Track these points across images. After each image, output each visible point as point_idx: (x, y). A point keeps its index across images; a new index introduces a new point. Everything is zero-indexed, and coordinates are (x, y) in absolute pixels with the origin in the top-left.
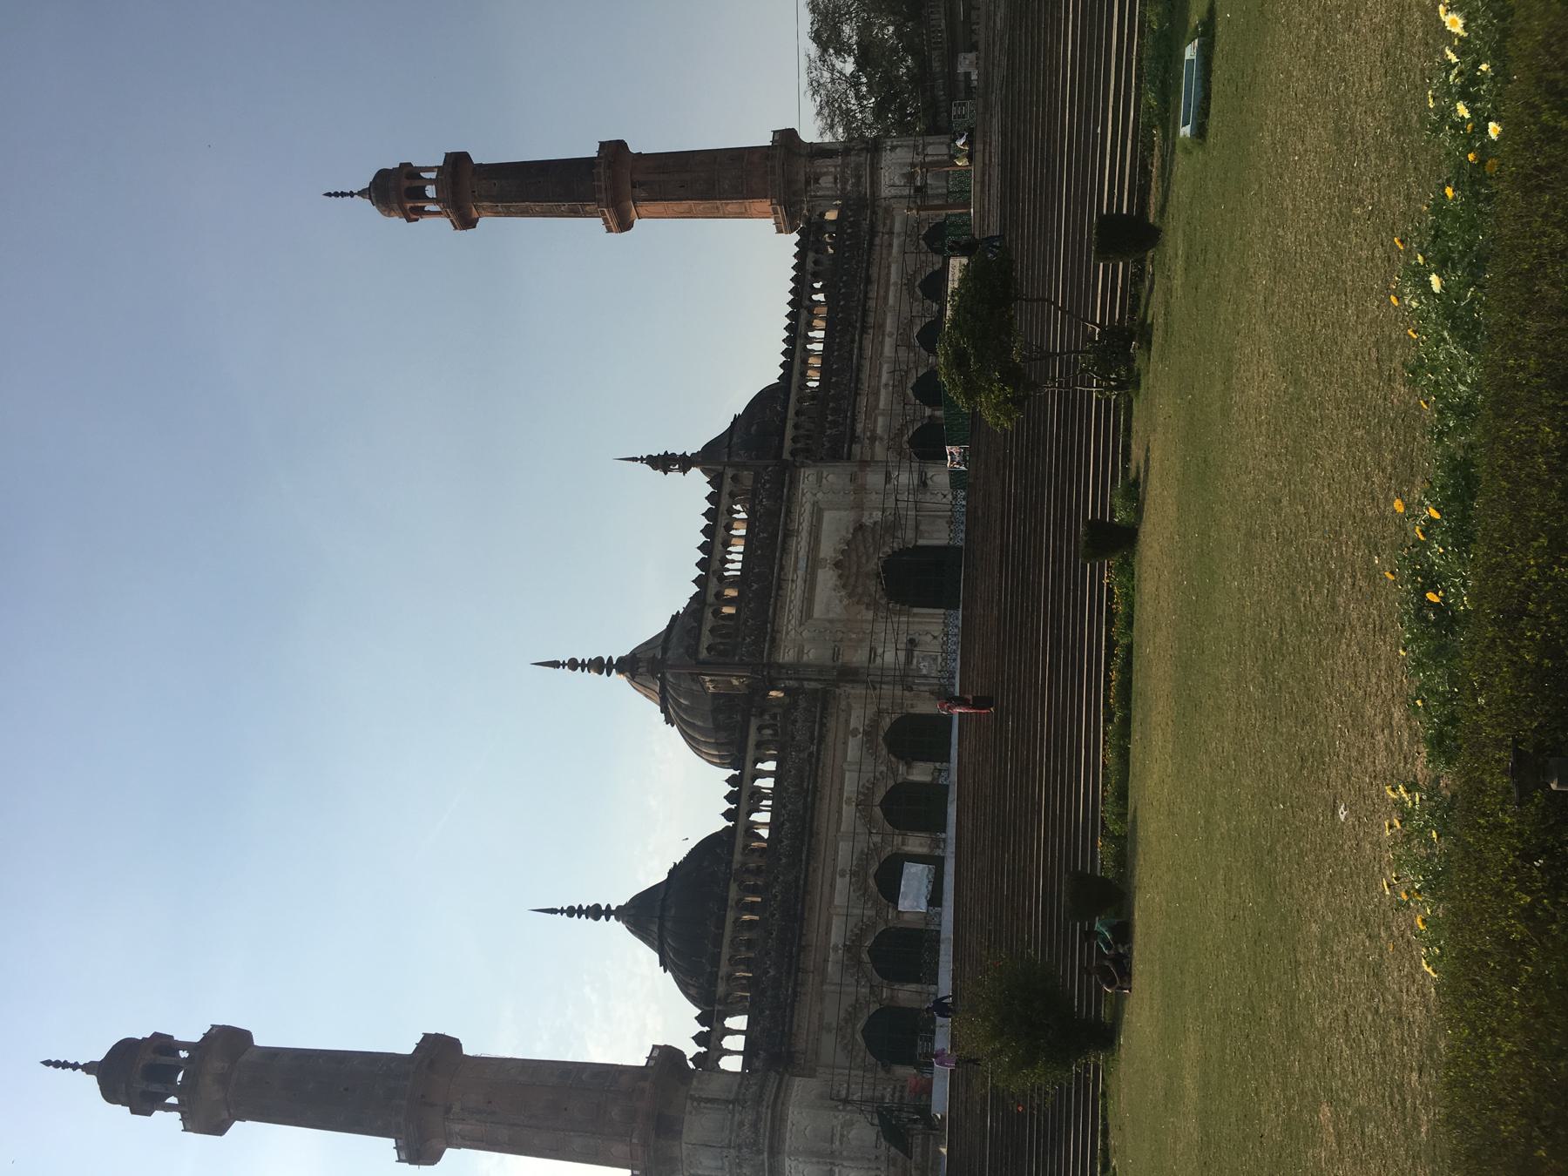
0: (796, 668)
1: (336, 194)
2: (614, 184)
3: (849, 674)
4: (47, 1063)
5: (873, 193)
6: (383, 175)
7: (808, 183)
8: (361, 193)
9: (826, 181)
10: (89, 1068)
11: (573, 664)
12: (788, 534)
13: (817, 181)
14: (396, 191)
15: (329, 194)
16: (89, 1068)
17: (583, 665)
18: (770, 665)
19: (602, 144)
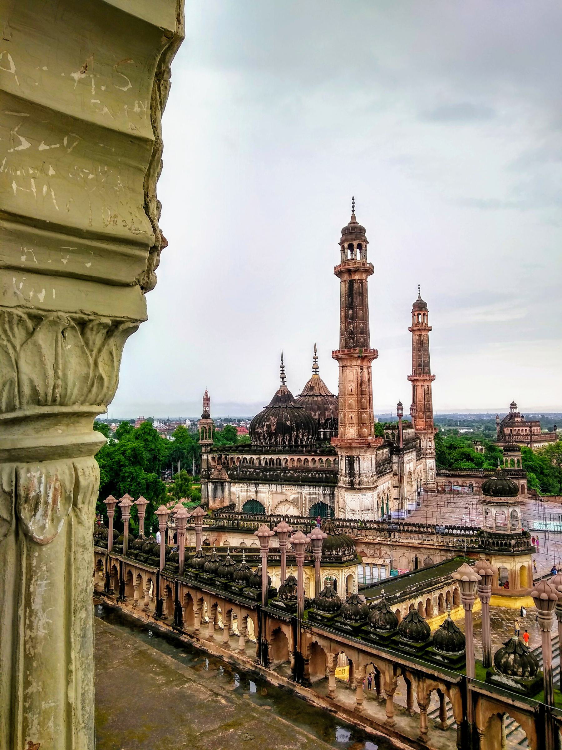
0: (401, 464)
3: (401, 480)
4: (353, 199)
5: (428, 458)
7: (430, 438)
8: (419, 297)
9: (429, 444)
10: (353, 217)
11: (315, 358)
16: (353, 217)
17: (315, 362)
18: (404, 454)
19: (434, 376)
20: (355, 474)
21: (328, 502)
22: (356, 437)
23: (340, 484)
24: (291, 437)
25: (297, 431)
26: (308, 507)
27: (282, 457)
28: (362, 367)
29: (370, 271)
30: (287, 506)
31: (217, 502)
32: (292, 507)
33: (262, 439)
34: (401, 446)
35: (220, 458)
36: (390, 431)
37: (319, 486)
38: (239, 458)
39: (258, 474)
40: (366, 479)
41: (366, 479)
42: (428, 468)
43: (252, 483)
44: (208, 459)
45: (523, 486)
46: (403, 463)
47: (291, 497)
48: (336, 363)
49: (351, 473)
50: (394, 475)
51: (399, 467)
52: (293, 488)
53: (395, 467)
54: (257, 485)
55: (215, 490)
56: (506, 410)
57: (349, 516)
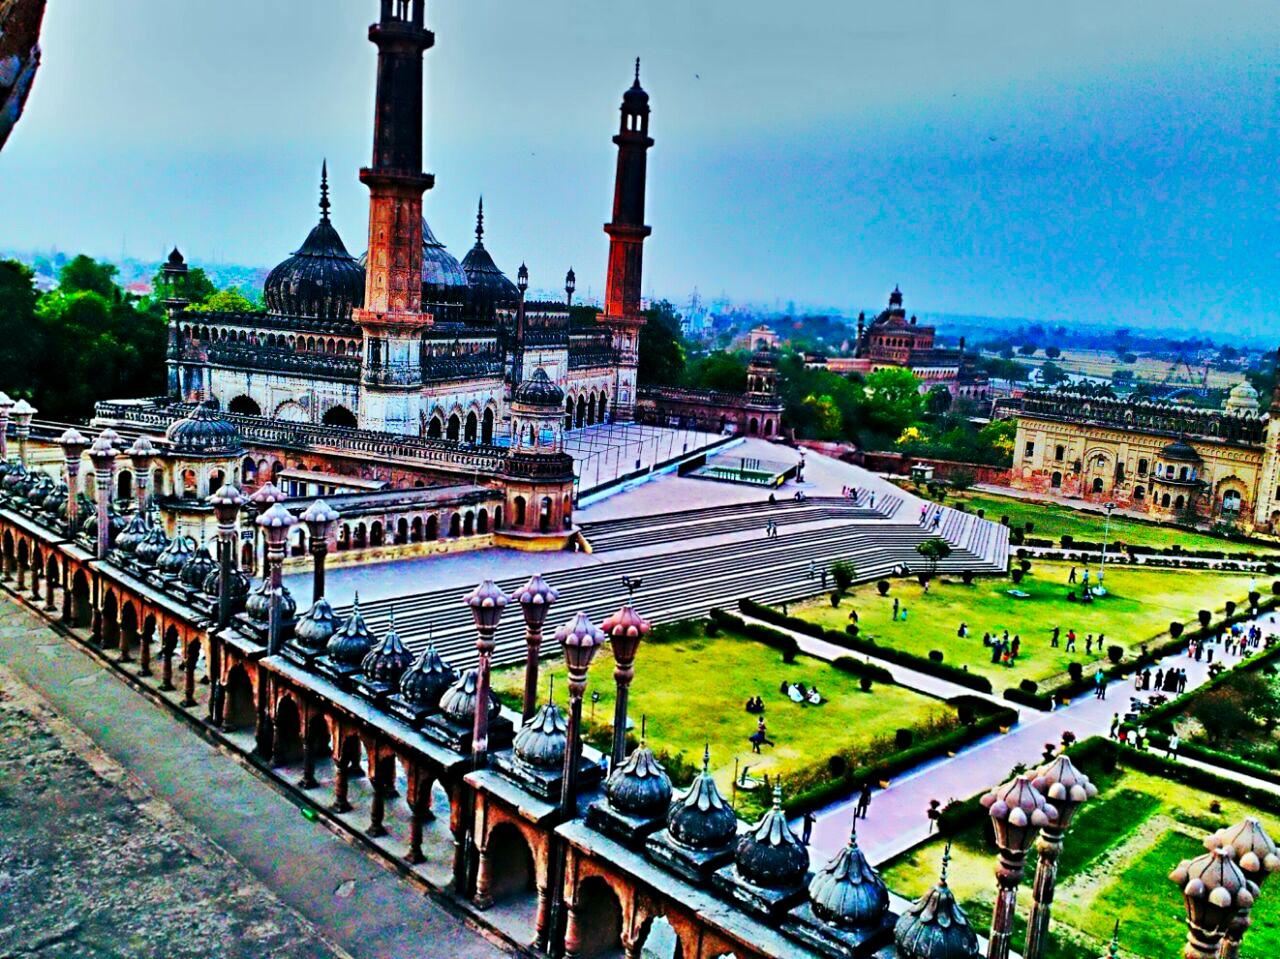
0: (518, 364)
1: (638, 65)
2: (628, 228)
6: (645, 97)
8: (637, 83)
9: (627, 341)
12: (553, 349)
13: (630, 339)
14: (636, 102)
15: (638, 60)
18: (523, 350)
20: (380, 366)
21: (349, 405)
22: (383, 309)
23: (363, 381)
24: (322, 304)
25: (333, 296)
26: (321, 413)
27: (287, 334)
28: (400, 200)
29: (428, 40)
30: (293, 409)
31: (192, 395)
32: (299, 411)
33: (277, 303)
34: (520, 335)
35: (196, 329)
36: (505, 312)
37: (338, 382)
38: (224, 331)
39: (251, 356)
40: (395, 375)
41: (395, 375)
42: (620, 383)
43: (242, 371)
44: (178, 327)
45: (770, 422)
46: (521, 364)
47: (296, 398)
48: (366, 190)
49: (375, 364)
50: (506, 382)
51: (514, 370)
52: (303, 381)
53: (508, 369)
54: (249, 373)
55: (188, 377)
56: (884, 305)
57: (371, 427)
